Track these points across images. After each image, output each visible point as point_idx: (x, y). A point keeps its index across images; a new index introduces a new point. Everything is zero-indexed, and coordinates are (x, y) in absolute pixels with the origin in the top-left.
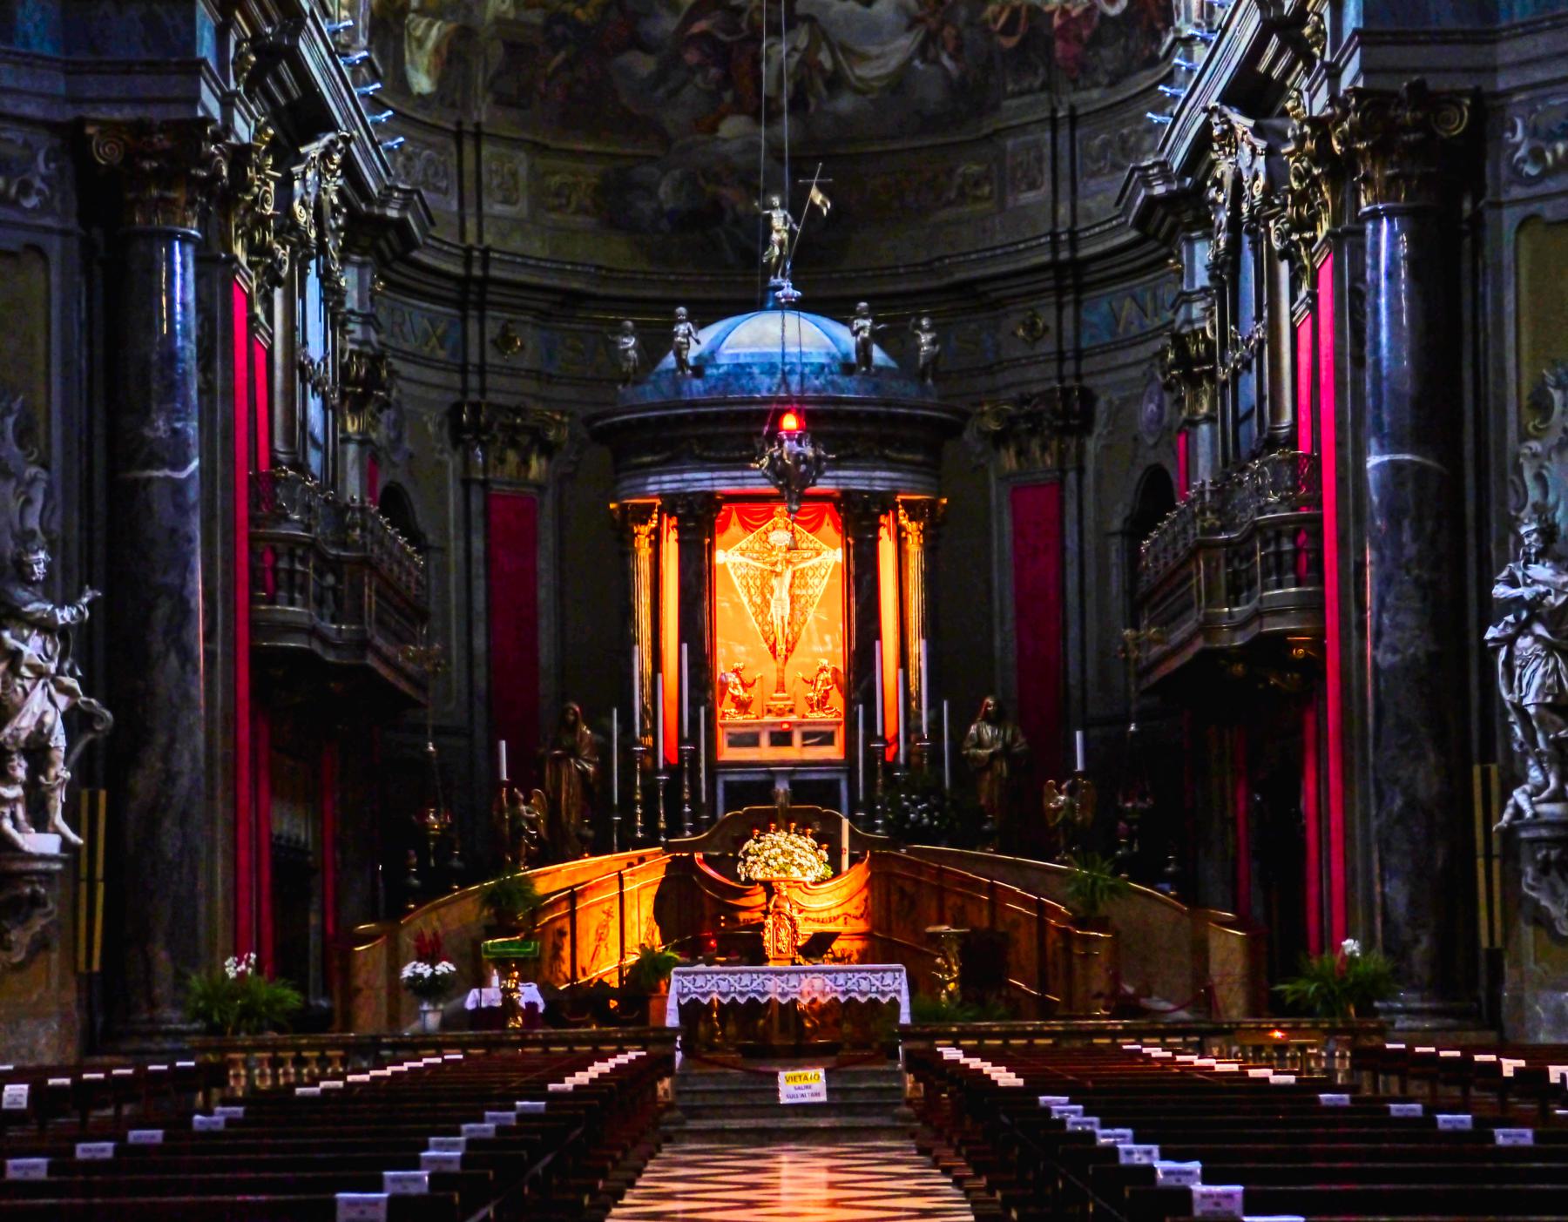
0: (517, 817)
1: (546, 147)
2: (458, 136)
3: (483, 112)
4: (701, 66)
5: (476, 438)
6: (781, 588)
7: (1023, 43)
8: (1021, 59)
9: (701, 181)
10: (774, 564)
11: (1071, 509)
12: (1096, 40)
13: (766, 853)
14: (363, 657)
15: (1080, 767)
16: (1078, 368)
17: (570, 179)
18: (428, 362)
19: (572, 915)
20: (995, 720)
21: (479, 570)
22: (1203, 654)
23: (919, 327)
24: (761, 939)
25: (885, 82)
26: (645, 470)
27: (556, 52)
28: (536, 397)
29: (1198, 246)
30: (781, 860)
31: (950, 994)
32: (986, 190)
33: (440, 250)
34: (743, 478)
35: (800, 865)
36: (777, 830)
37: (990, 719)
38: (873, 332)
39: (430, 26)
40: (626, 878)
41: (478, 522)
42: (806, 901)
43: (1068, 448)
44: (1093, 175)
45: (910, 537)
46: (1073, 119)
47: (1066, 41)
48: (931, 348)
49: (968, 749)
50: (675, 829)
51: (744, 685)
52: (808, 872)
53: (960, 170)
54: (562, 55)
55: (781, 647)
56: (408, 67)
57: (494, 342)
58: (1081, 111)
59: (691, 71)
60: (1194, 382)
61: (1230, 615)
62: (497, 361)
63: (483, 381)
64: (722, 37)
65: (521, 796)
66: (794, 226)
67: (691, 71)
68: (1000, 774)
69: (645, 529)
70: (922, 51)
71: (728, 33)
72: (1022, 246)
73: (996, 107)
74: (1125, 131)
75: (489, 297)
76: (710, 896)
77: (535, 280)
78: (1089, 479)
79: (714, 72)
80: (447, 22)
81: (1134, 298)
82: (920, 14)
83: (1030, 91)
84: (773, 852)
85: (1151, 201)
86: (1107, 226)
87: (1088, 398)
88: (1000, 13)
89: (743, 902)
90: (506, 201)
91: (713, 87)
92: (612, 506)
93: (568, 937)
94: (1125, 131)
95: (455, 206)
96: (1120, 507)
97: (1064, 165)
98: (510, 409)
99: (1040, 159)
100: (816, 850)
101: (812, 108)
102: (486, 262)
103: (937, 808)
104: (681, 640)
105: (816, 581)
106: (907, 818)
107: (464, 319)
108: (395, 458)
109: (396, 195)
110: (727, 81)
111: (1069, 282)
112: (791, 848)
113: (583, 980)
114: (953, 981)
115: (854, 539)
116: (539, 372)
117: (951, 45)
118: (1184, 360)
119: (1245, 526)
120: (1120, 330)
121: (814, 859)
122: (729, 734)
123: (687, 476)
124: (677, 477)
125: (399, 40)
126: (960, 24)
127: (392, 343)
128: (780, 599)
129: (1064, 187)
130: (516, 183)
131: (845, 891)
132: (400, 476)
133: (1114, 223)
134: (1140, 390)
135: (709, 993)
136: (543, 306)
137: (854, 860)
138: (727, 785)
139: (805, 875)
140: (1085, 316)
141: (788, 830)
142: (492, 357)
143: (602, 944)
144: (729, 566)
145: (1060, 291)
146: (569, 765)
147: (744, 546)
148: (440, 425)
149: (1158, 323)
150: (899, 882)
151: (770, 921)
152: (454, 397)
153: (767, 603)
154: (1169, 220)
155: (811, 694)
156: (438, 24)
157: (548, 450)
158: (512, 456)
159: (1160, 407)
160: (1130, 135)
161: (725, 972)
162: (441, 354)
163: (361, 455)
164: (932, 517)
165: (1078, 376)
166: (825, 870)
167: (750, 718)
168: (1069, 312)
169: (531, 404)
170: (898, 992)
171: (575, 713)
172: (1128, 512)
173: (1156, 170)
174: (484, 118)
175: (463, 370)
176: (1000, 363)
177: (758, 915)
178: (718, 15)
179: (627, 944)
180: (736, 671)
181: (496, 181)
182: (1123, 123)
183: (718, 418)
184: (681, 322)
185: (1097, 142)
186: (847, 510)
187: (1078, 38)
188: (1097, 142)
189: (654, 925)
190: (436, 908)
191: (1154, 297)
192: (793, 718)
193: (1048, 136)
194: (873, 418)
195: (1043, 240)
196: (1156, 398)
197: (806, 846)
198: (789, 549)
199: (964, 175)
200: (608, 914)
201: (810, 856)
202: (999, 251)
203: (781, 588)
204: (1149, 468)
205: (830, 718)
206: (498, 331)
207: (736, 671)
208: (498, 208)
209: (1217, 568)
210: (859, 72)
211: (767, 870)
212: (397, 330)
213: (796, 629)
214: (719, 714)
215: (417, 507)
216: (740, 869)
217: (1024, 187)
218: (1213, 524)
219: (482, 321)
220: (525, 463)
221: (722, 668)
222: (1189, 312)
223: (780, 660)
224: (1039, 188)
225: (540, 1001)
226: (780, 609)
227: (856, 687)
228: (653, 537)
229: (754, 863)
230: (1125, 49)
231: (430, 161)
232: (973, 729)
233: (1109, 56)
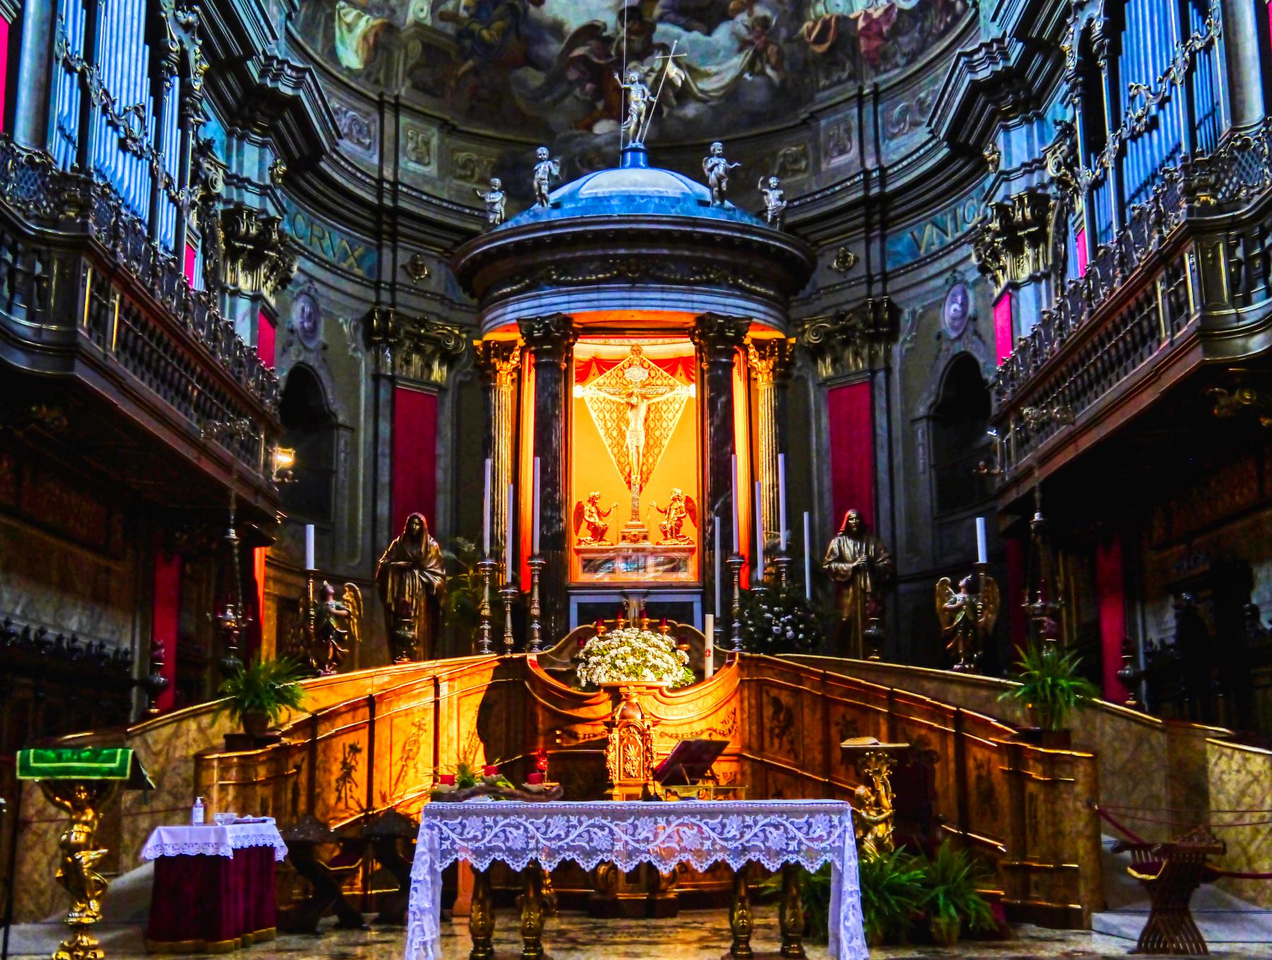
0: (323, 613)
1: (454, 128)
2: (380, 105)
3: (403, 90)
4: (580, 82)
5: (386, 341)
6: (636, 420)
7: (832, 48)
8: (831, 60)
9: (578, 165)
10: (630, 395)
11: (881, 402)
12: (896, 31)
13: (613, 653)
14: (72, 368)
15: (982, 559)
16: (884, 288)
17: (475, 157)
18: (346, 275)
19: (372, 724)
20: (856, 534)
21: (384, 449)
22: (1202, 368)
23: (769, 187)
24: (604, 759)
25: (721, 93)
26: (504, 300)
27: (466, 60)
28: (440, 317)
29: (1014, 134)
30: (631, 660)
31: (879, 842)
32: (803, 164)
33: (354, 175)
34: (599, 300)
35: (655, 668)
36: (627, 625)
37: (849, 533)
38: (726, 170)
39: (359, 17)
40: (444, 687)
41: (385, 412)
42: (662, 712)
43: (877, 353)
44: (894, 136)
45: (759, 376)
46: (877, 95)
47: (868, 38)
48: (779, 203)
49: (830, 563)
50: (522, 642)
51: (599, 514)
52: (665, 676)
53: (781, 153)
54: (470, 63)
55: (635, 478)
56: (338, 43)
57: (403, 267)
58: (882, 88)
59: (572, 84)
60: (1015, 248)
61: (1239, 317)
62: (408, 281)
63: (393, 298)
64: (596, 60)
65: (331, 589)
66: (652, 99)
67: (572, 84)
68: (864, 591)
69: (508, 367)
70: (750, 66)
71: (599, 57)
72: (837, 188)
73: (811, 100)
74: (922, 95)
75: (400, 228)
76: (544, 707)
77: (439, 218)
78: (896, 376)
79: (589, 86)
80: (376, 18)
81: (935, 224)
82: (749, 37)
83: (840, 82)
84: (621, 650)
85: (975, 87)
86: (914, 157)
87: (895, 311)
88: (813, 28)
89: (582, 713)
90: (418, 161)
91: (588, 98)
92: (476, 343)
93: (365, 754)
94: (922, 95)
95: (376, 160)
96: (925, 395)
97: (869, 132)
98: (415, 320)
99: (848, 131)
100: (674, 650)
101: (665, 115)
102: (395, 195)
103: (801, 620)
104: (535, 455)
105: (671, 416)
106: (770, 633)
107: (379, 248)
108: (311, 345)
109: (289, 72)
110: (599, 94)
111: (877, 217)
112: (644, 646)
113: (380, 807)
114: (885, 821)
115: (709, 363)
116: (443, 297)
117: (773, 60)
118: (1009, 227)
119: (1256, 199)
120: (922, 251)
121: (671, 660)
122: (584, 560)
123: (544, 301)
124: (536, 303)
125: (331, 18)
126: (781, 41)
127: (310, 248)
128: (635, 430)
129: (870, 148)
130: (428, 151)
131: (710, 701)
132: (313, 361)
133: (922, 151)
134: (943, 295)
135: (491, 850)
136: (449, 244)
137: (720, 660)
138: (580, 605)
139: (660, 679)
140: (888, 247)
141: (640, 626)
142: (401, 277)
143: (411, 764)
144: (587, 400)
145: (869, 227)
146: (413, 576)
147: (601, 382)
148: (356, 328)
149: (958, 234)
150: (774, 692)
151: (615, 735)
152: (366, 308)
153: (622, 435)
154: (989, 108)
155: (665, 523)
156: (367, 17)
157: (449, 359)
158: (416, 358)
159: (964, 304)
160: (927, 96)
161: (518, 813)
162: (357, 271)
163: (253, 310)
164: (782, 356)
165: (885, 293)
166: (682, 674)
167: (605, 545)
168: (876, 247)
169: (434, 320)
170: (840, 851)
171: (421, 523)
172: (932, 399)
173: (981, 54)
174: (403, 92)
175: (377, 287)
176: (818, 291)
177: (602, 728)
178: (593, 43)
179: (441, 764)
180: (592, 501)
181: (410, 146)
182: (921, 90)
183: (577, 240)
184: (541, 161)
185: (898, 109)
186: (701, 336)
187: (880, 33)
188: (898, 109)
189: (477, 741)
190: (195, 715)
191: (955, 218)
192: (647, 544)
193: (855, 111)
194: (728, 242)
195: (857, 179)
196: (959, 298)
197: (662, 645)
198: (644, 386)
199: (785, 155)
200: (419, 727)
201: (667, 657)
202: (817, 196)
203: (636, 420)
204: (955, 357)
205: (682, 545)
206: (407, 260)
207: (592, 501)
208: (412, 166)
209: (1216, 258)
210: (700, 85)
211: (614, 673)
212: (315, 240)
213: (651, 460)
214: (575, 539)
215: (329, 391)
216: (581, 672)
217: (835, 154)
218: (1207, 202)
219: (394, 251)
220: (428, 367)
221: (578, 493)
222: (1009, 188)
223: (636, 488)
224: (848, 152)
225: (279, 842)
226: (635, 437)
227: (711, 507)
228: (515, 375)
229: (598, 664)
230: (921, 31)
231: (354, 119)
232: (834, 544)
233: (907, 42)
